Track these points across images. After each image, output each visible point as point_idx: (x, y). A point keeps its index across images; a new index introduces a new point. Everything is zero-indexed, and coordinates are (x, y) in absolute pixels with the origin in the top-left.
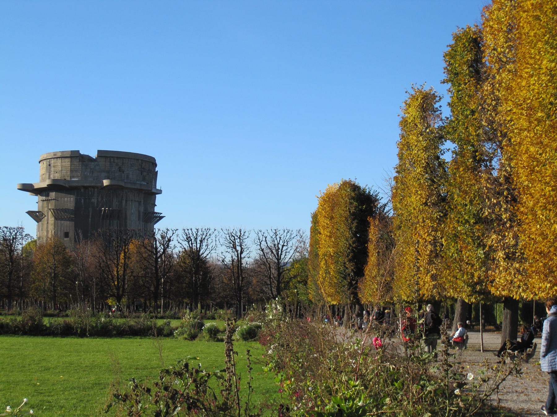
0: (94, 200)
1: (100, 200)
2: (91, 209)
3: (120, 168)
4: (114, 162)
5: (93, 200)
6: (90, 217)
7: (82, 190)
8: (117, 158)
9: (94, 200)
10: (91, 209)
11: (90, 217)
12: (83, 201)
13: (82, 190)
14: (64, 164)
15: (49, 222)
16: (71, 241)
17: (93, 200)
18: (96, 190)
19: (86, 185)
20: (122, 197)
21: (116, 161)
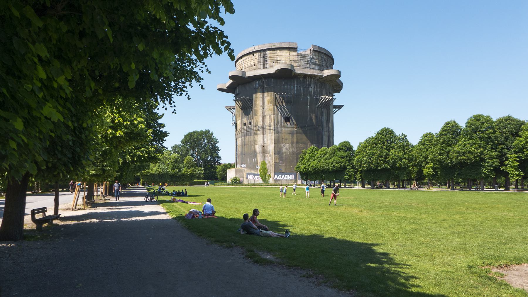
0: (311, 89)
2: (309, 97)
5: (310, 89)
8: (325, 54)
9: (311, 89)
10: (309, 97)
14: (282, 54)
15: (265, 108)
17: (310, 89)
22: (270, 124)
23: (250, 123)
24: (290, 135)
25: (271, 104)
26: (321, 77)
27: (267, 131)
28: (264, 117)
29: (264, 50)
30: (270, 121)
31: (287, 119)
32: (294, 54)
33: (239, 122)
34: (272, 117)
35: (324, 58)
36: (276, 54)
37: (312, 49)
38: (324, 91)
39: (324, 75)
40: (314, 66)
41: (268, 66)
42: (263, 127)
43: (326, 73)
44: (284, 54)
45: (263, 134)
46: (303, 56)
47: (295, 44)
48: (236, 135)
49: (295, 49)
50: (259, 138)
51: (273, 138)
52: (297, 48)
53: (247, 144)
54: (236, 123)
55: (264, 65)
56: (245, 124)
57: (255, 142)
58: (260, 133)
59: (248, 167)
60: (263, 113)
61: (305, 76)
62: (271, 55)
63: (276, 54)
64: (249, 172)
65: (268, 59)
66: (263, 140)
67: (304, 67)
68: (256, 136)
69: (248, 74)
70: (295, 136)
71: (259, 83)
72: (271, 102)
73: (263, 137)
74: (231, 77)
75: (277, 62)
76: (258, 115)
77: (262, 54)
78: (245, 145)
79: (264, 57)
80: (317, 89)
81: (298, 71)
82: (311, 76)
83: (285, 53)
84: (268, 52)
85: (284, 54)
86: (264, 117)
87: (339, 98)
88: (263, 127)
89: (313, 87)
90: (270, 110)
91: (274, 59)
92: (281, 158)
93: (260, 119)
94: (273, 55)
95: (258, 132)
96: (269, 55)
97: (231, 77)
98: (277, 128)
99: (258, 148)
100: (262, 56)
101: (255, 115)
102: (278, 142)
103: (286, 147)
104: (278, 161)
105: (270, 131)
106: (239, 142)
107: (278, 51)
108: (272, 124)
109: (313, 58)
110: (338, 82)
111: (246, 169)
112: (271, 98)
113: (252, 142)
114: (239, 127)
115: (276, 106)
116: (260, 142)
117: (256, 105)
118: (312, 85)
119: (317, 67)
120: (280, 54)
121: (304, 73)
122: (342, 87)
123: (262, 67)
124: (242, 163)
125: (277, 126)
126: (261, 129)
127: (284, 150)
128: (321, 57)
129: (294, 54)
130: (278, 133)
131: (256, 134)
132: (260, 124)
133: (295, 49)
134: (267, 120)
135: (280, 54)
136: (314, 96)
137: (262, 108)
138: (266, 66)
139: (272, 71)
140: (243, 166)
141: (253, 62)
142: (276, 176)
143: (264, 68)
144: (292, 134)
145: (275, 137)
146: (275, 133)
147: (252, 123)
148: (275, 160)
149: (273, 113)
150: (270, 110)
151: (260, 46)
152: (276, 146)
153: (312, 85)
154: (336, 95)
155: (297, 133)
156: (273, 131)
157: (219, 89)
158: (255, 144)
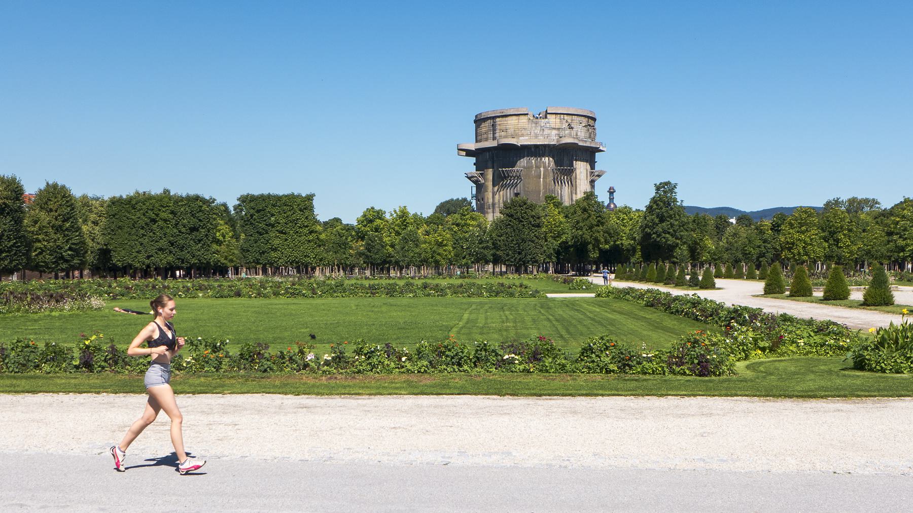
2: (542, 169)
10: (542, 169)
29: (494, 118)
32: (523, 119)
38: (565, 159)
41: (497, 135)
42: (494, 204)
61: (536, 146)
65: (498, 127)
82: (544, 146)
83: (512, 121)
88: (494, 204)
91: (503, 127)
93: (491, 195)
108: (501, 201)
132: (491, 201)
139: (494, 144)
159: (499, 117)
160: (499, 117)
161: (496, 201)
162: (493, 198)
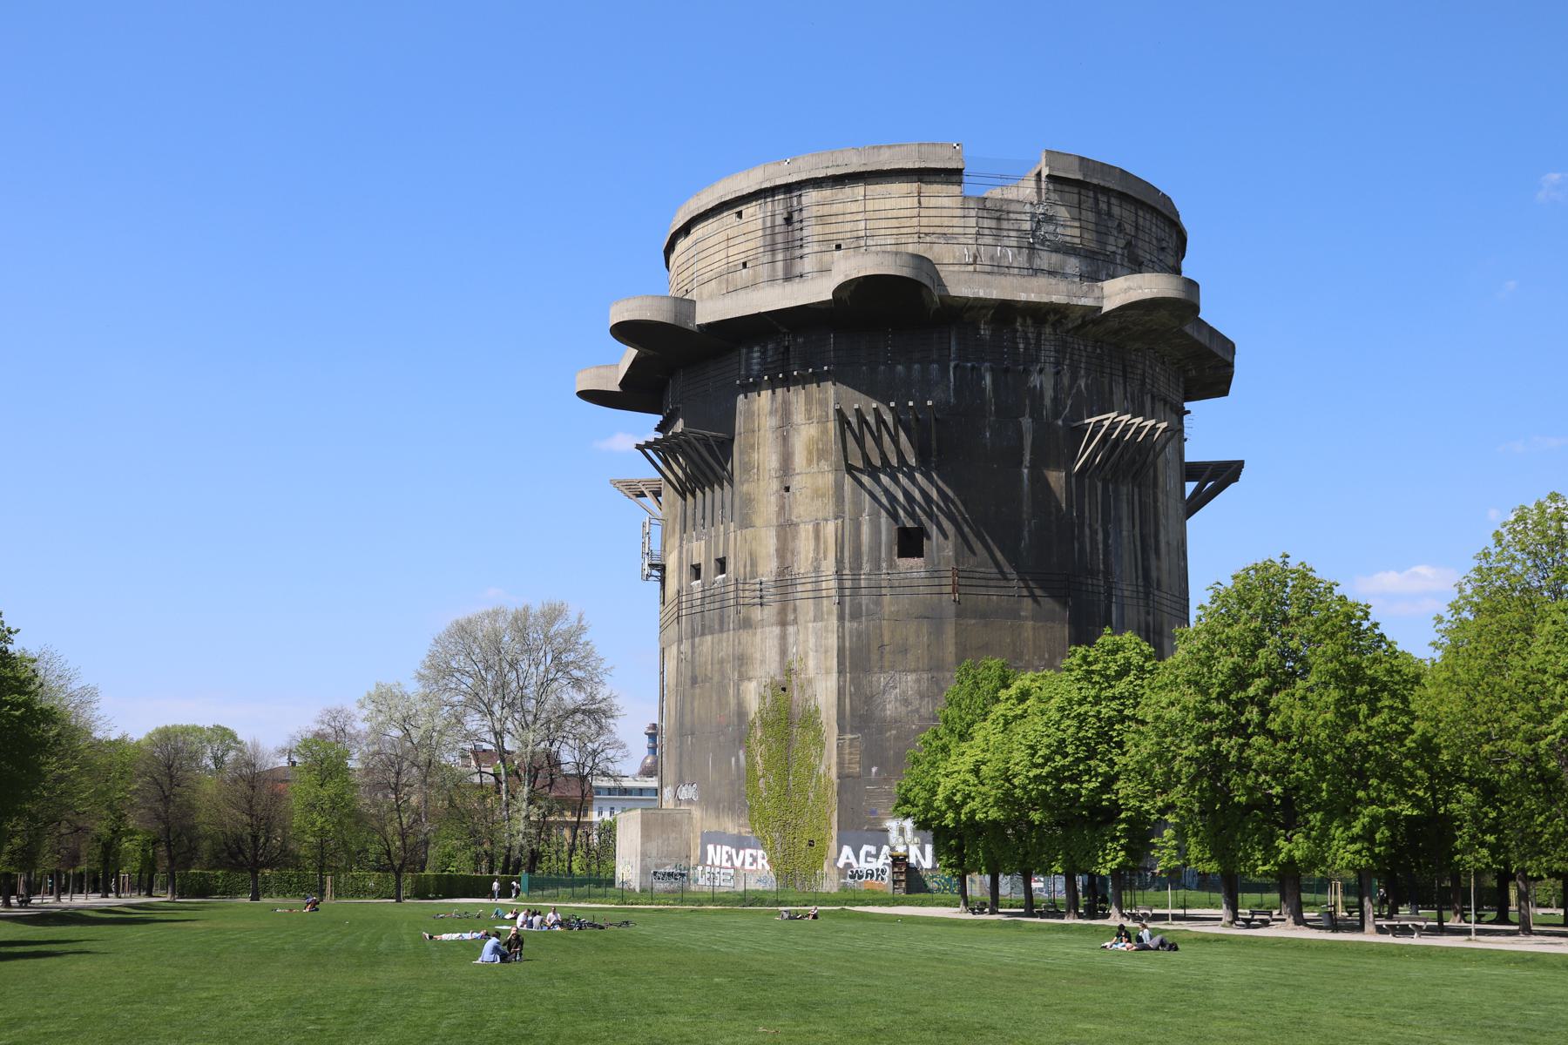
0: (1042, 381)
1: (1066, 381)
2: (1026, 422)
3: (1129, 244)
4: (1109, 214)
5: (1035, 380)
6: (1027, 457)
7: (985, 331)
8: (1123, 197)
10: (1026, 422)
11: (1027, 457)
12: (988, 379)
13: (985, 331)
15: (796, 483)
16: (934, 573)
17: (1035, 380)
18: (1048, 330)
19: (1023, 297)
20: (1143, 383)
21: (1116, 211)
22: (817, 569)
23: (722, 565)
24: (925, 626)
25: (825, 466)
26: (1092, 318)
27: (806, 608)
28: (786, 529)
29: (788, 188)
30: (815, 554)
31: (910, 543)
32: (942, 197)
33: (672, 563)
34: (830, 529)
35: (1122, 215)
36: (854, 207)
37: (1044, 174)
38: (1118, 393)
39: (1107, 307)
40: (1056, 258)
41: (808, 265)
43: (1119, 291)
44: (889, 204)
45: (783, 624)
46: (997, 213)
47: (948, 152)
48: (663, 628)
49: (951, 175)
50: (764, 645)
51: (833, 641)
52: (959, 172)
53: (706, 679)
54: (663, 568)
55: (789, 263)
56: (696, 571)
57: (742, 661)
58: (770, 612)
59: (709, 801)
60: (782, 508)
61: (1005, 311)
62: (826, 210)
63: (854, 207)
64: (712, 825)
65: (811, 231)
66: (783, 652)
67: (999, 268)
68: (745, 635)
69: (706, 314)
70: (950, 631)
71: (764, 353)
72: (822, 455)
73: (783, 638)
74: (625, 332)
75: (859, 243)
76: (758, 521)
77: (778, 205)
78: (694, 681)
79: (788, 220)
80: (1074, 378)
81: (963, 285)
82: (1039, 313)
83: (896, 198)
84: (811, 196)
85: (889, 204)
86: (786, 529)
87: (1207, 430)
89: (1050, 370)
90: (817, 494)
92: (874, 753)
93: (768, 542)
94: (836, 208)
95: (757, 614)
96: (815, 211)
97: (625, 332)
98: (856, 589)
99: (753, 696)
100: (779, 220)
101: (746, 523)
102: (856, 661)
103: (899, 692)
104: (856, 769)
105: (818, 608)
106: (671, 665)
107: (859, 190)
108: (829, 566)
109: (1050, 219)
110: (1204, 339)
111: (697, 813)
112: (825, 432)
113: (728, 667)
114: (672, 584)
115: (850, 469)
116: (766, 665)
117: (747, 468)
118: (1048, 354)
119: (1073, 265)
120: (870, 205)
121: (995, 294)
122: (1231, 365)
123: (780, 274)
124: (680, 781)
125: (856, 577)
126: (771, 595)
127: (891, 708)
128: (1098, 213)
129: (946, 202)
130: (856, 615)
131: (746, 624)
132: (768, 568)
133: (951, 175)
134: (804, 545)
135: (870, 205)
136: (1057, 415)
137: (775, 485)
138: (799, 267)
139: (817, 290)
140: (686, 792)
141: (737, 252)
142: (847, 850)
143: (788, 278)
144: (932, 617)
145: (841, 638)
146: (841, 618)
147: (730, 567)
148: (840, 764)
149: (831, 509)
150: (817, 494)
151: (771, 168)
152: (849, 689)
153: (1048, 354)
154: (1200, 414)
155: (958, 615)
156: (830, 606)
157: (584, 395)
158: (743, 677)
159: (816, 183)
160: (816, 183)
161: (803, 562)
162: (784, 551)
